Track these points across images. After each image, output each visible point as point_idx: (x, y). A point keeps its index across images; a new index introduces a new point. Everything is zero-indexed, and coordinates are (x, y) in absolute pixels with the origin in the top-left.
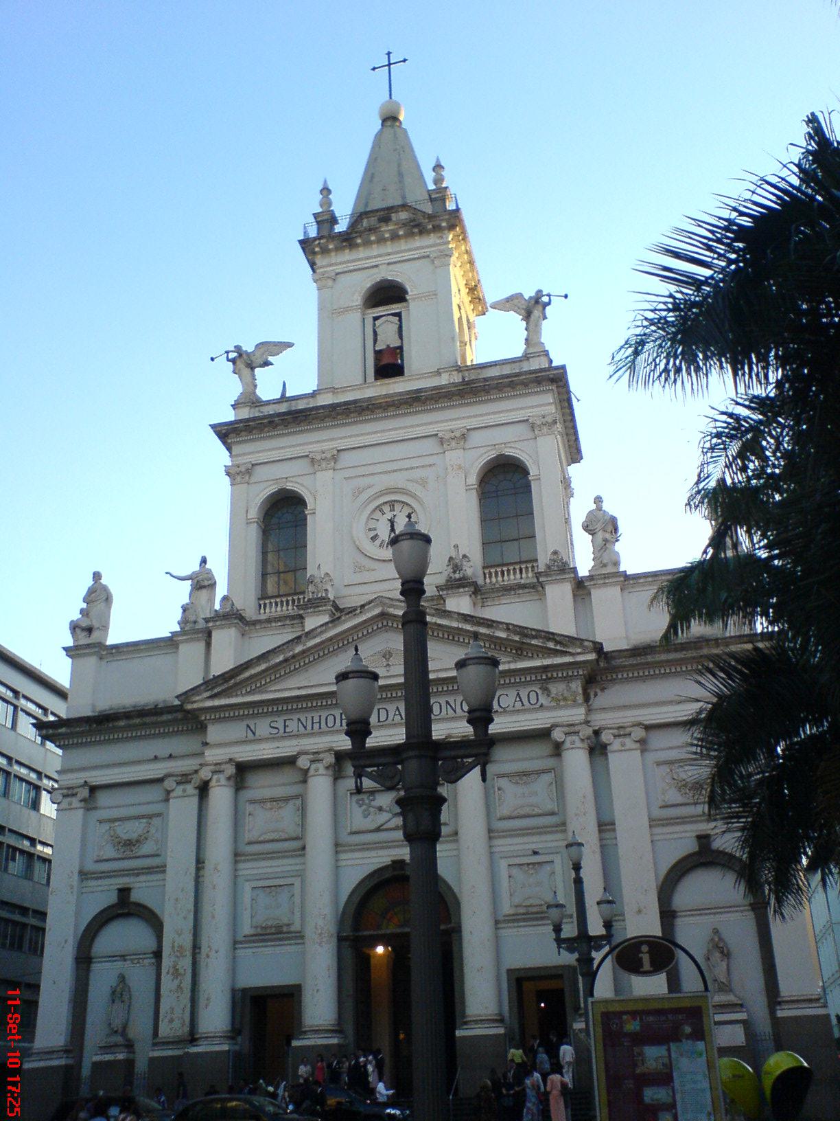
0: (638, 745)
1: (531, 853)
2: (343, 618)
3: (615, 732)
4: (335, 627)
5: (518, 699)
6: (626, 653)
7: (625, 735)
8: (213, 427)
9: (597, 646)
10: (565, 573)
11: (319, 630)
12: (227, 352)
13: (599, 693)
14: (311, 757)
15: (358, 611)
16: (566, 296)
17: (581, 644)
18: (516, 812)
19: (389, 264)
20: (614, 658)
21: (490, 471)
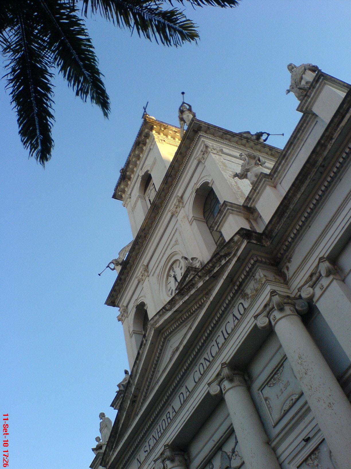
0: (331, 277)
1: (304, 443)
2: (141, 352)
3: (311, 283)
4: (140, 360)
5: (235, 318)
6: (275, 219)
7: (318, 279)
8: (106, 303)
9: (241, 233)
10: (223, 212)
11: (135, 369)
12: (108, 266)
13: (288, 264)
14: (160, 460)
15: (144, 342)
16: (183, 93)
17: (234, 242)
18: (283, 411)
19: (141, 169)
20: (271, 231)
21: (205, 204)
